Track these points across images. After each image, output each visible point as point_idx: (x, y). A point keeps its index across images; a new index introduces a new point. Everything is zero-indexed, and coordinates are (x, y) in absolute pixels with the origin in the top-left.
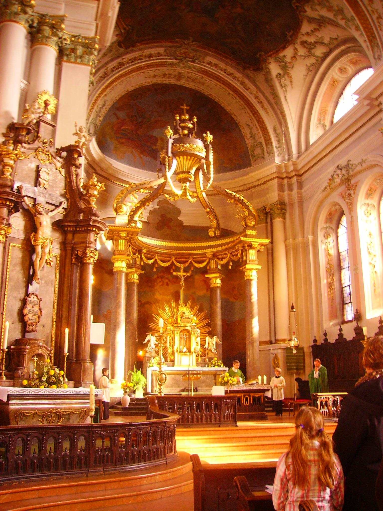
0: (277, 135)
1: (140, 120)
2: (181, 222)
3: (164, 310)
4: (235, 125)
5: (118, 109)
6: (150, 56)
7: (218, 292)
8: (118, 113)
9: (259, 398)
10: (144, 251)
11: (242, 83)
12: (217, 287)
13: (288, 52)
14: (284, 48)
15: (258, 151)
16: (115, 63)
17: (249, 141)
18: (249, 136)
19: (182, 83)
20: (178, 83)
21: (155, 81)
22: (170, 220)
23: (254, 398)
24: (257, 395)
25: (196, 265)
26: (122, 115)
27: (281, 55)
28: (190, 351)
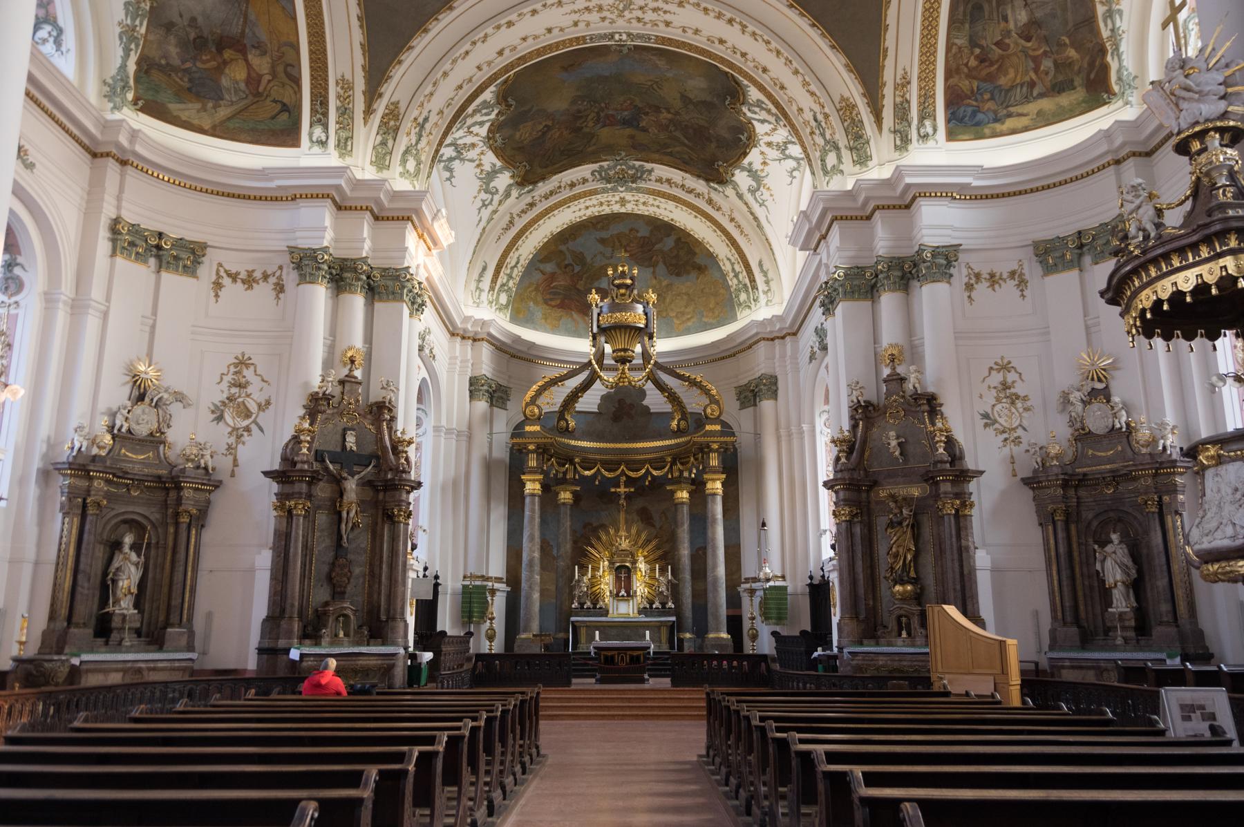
0: (765, 273)
1: (577, 268)
2: (647, 408)
3: (599, 539)
4: (712, 257)
5: (541, 261)
6: (572, 185)
7: (685, 509)
8: (542, 266)
9: (638, 657)
10: (577, 460)
11: (710, 202)
12: (683, 503)
13: (754, 157)
14: (745, 154)
15: (743, 297)
16: (522, 205)
17: (733, 282)
18: (732, 275)
19: (629, 208)
20: (623, 210)
21: (589, 213)
22: (632, 406)
23: (632, 657)
24: (635, 653)
25: (655, 473)
26: (549, 268)
27: (746, 162)
28: (629, 595)
